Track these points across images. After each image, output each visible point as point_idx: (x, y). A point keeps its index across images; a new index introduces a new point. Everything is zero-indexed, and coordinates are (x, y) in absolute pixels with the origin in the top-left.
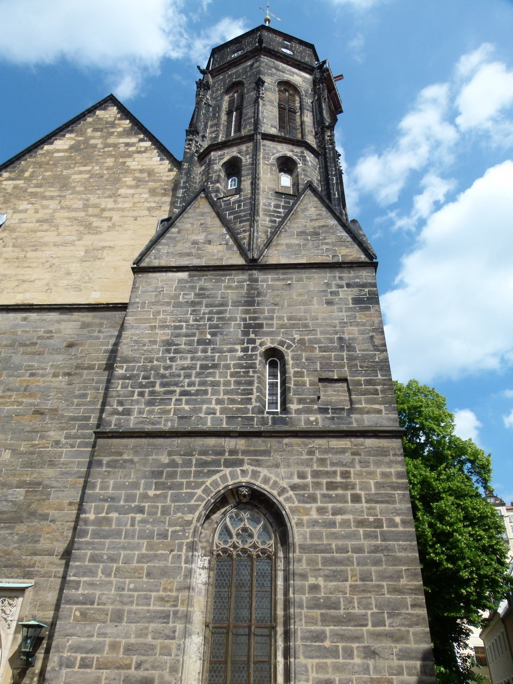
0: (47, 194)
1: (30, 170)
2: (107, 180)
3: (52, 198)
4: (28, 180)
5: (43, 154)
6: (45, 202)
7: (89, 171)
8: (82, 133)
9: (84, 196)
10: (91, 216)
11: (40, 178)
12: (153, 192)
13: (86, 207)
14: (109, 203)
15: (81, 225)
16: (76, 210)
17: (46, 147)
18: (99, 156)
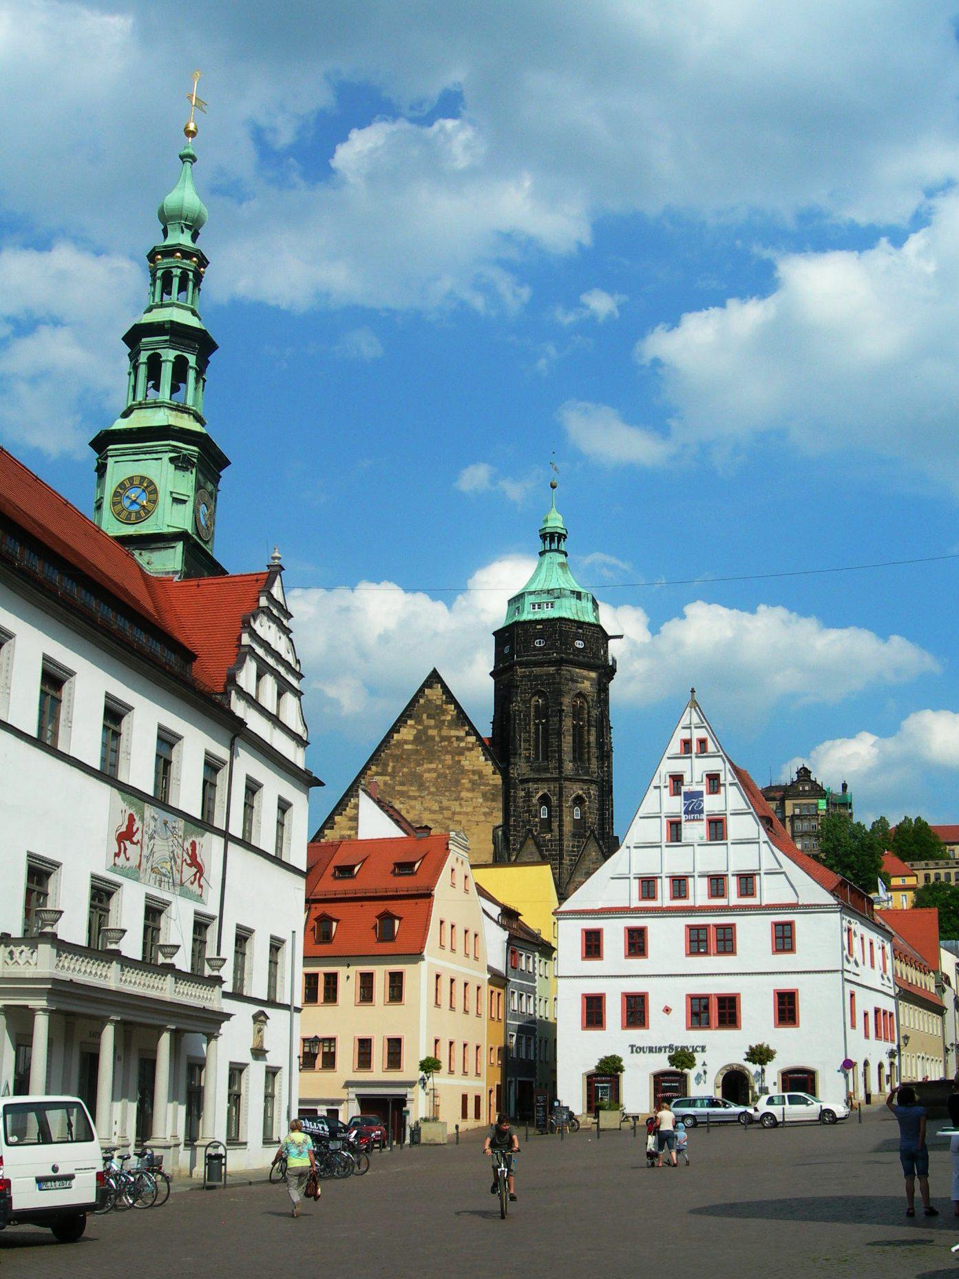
0: (411, 793)
1: (391, 764)
2: (450, 781)
3: (415, 798)
4: (393, 775)
5: (395, 745)
6: (413, 803)
7: (435, 770)
8: (419, 721)
9: (437, 798)
10: (446, 819)
11: (401, 774)
12: (484, 795)
13: (442, 809)
14: (455, 807)
15: (442, 827)
16: (434, 812)
17: (396, 736)
18: (440, 751)
